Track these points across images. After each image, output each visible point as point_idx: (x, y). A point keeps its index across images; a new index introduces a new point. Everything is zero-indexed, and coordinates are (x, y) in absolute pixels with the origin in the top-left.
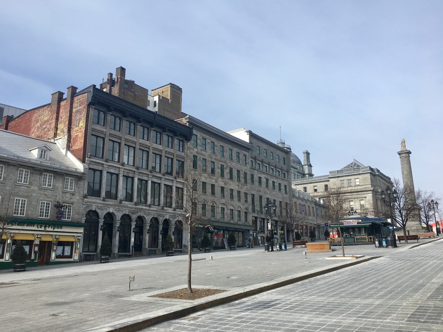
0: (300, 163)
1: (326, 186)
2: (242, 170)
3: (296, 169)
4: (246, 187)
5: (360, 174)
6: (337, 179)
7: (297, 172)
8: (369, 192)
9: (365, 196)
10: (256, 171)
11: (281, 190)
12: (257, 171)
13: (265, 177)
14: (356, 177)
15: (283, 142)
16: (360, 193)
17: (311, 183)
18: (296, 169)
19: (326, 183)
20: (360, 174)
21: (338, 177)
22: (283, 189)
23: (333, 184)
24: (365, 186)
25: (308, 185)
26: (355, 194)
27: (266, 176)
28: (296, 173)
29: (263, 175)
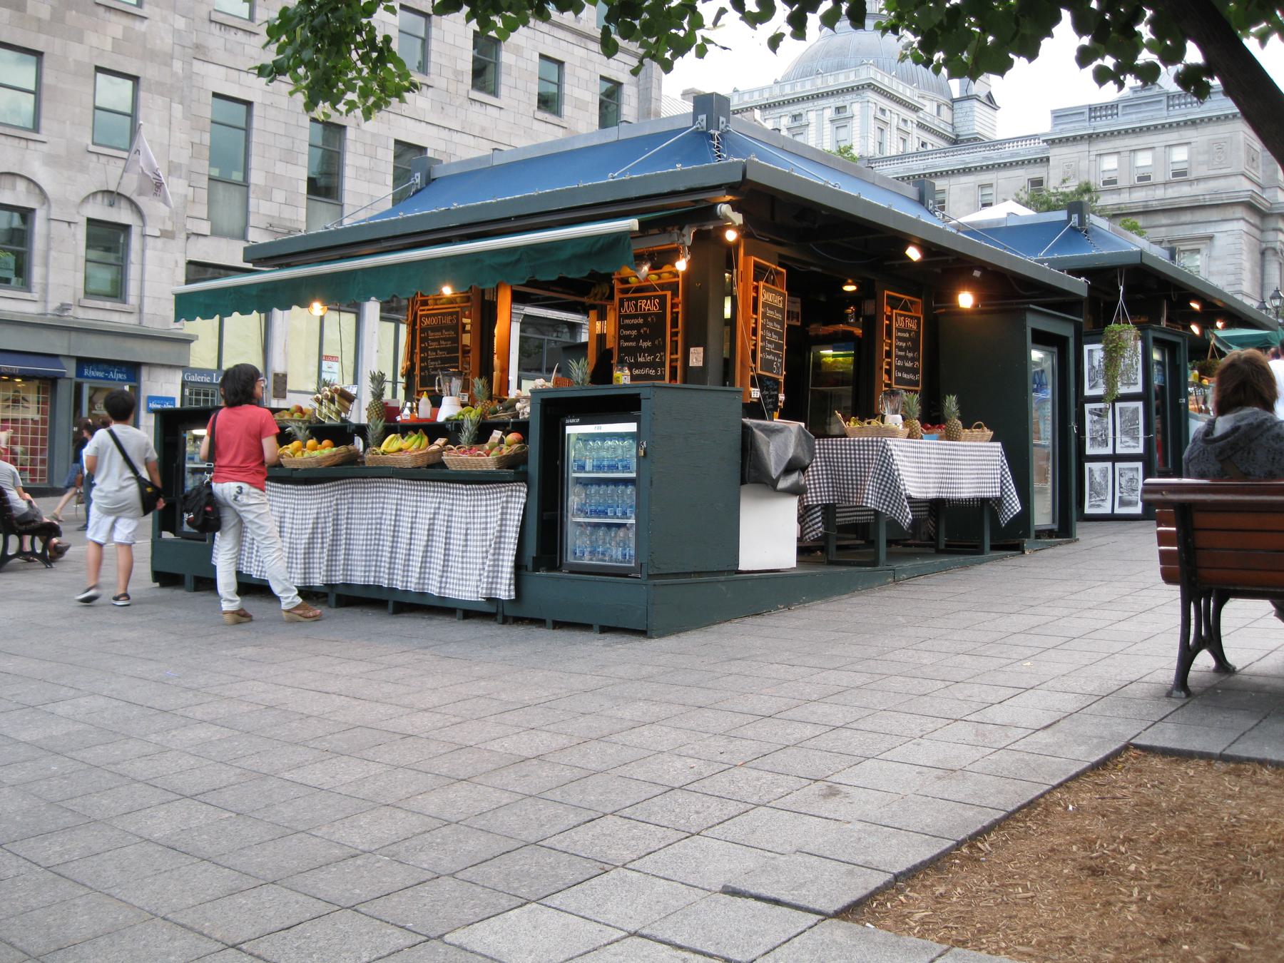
1: (1037, 183)
3: (915, 109)
6: (1083, 147)
7: (921, 126)
8: (1229, 213)
9: (1209, 230)
11: (567, 109)
14: (1172, 137)
16: (1187, 217)
17: (966, 171)
18: (915, 109)
19: (1036, 172)
21: (1091, 138)
22: (580, 105)
23: (1064, 173)
24: (1213, 185)
25: (953, 180)
26: (1164, 220)
28: (911, 128)
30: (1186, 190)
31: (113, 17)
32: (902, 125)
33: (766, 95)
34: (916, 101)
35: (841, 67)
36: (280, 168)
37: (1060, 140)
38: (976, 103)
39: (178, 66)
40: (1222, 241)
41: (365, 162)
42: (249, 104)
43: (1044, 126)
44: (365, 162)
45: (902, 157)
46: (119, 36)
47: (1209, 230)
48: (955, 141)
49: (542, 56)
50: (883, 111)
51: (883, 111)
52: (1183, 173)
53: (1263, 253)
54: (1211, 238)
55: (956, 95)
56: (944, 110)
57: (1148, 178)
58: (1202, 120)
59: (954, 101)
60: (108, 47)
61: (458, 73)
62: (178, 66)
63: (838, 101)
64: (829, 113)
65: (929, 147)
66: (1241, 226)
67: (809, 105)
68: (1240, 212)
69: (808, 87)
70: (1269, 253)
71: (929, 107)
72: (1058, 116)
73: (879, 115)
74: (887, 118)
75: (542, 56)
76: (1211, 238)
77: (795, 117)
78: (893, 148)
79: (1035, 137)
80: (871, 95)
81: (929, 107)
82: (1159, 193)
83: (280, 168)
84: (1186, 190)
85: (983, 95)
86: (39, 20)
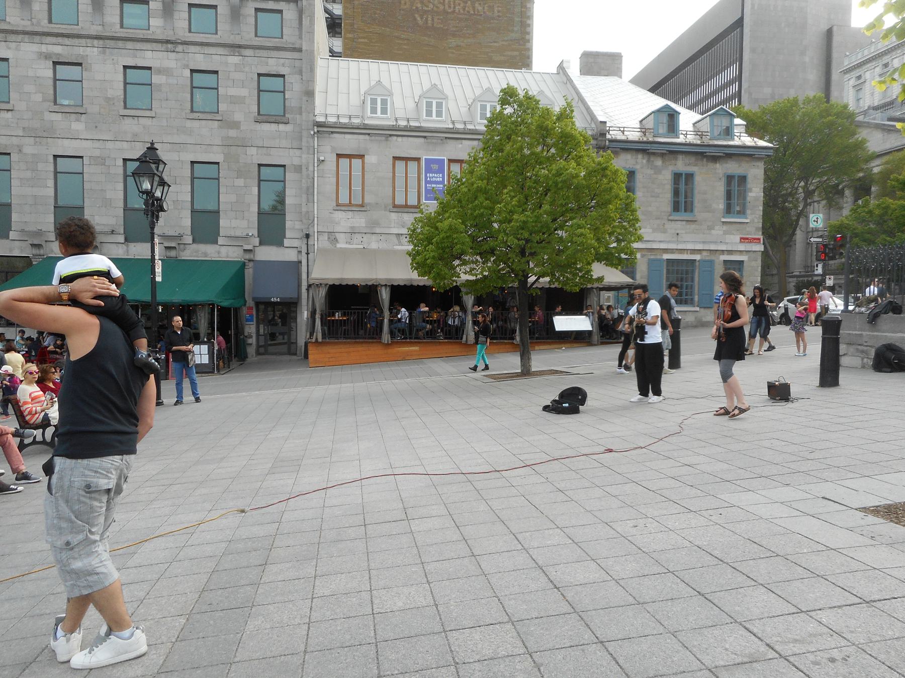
13: (47, 56)
27: (58, 49)
29: (35, 48)
41: (28, 174)
44: (28, 174)
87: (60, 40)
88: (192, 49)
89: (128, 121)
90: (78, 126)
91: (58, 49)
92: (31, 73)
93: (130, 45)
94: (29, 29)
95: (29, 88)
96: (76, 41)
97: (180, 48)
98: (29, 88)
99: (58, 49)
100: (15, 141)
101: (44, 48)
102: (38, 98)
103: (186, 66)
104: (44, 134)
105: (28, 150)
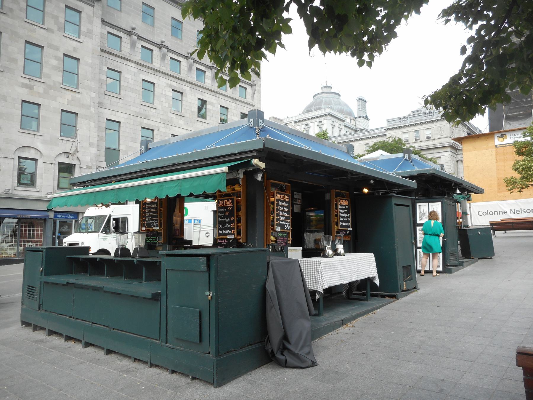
0: (350, 114)
2: (57, 49)
3: (344, 121)
4: (69, 95)
5: (432, 121)
6: (397, 130)
7: (345, 126)
8: (445, 150)
9: (439, 155)
10: (133, 65)
12: (137, 63)
13: (170, 86)
15: (328, 85)
16: (432, 151)
18: (344, 121)
20: (432, 121)
27: (174, 84)
28: (343, 127)
30: (431, 143)
31: (67, 92)
32: (339, 126)
33: (297, 118)
34: (344, 119)
35: (320, 109)
36: (131, 144)
37: (390, 129)
38: (362, 118)
39: (92, 109)
40: (443, 158)
42: (119, 122)
43: (385, 125)
45: (340, 136)
46: (70, 99)
47: (439, 155)
48: (356, 131)
49: (221, 106)
50: (333, 122)
51: (333, 122)
52: (430, 138)
53: (457, 162)
54: (440, 158)
55: (356, 116)
56: (352, 120)
57: (419, 139)
58: (435, 120)
59: (355, 118)
60: (66, 103)
61: (192, 112)
62: (92, 109)
63: (319, 120)
64: (317, 123)
65: (348, 133)
66: (449, 153)
67: (310, 121)
68: (449, 149)
69: (309, 115)
70: (459, 162)
71: (348, 120)
72: (389, 121)
73: (332, 123)
74: (335, 124)
75: (221, 106)
76: (440, 158)
77: (307, 125)
78: (336, 133)
79: (381, 128)
80: (329, 117)
81: (348, 120)
82: (422, 144)
83: (131, 144)
84: (431, 143)
85: (364, 116)
86: (39, 93)
87: (176, 80)
88: (221, 96)
89: (199, 123)
90: (181, 122)
91: (176, 84)
92: (164, 93)
93: (201, 89)
94: (165, 72)
95: (163, 99)
96: (184, 83)
97: (217, 95)
98: (163, 99)
99: (174, 84)
100: (157, 124)
101: (169, 82)
102: (166, 105)
103: (219, 103)
104: (168, 123)
105: (161, 130)
